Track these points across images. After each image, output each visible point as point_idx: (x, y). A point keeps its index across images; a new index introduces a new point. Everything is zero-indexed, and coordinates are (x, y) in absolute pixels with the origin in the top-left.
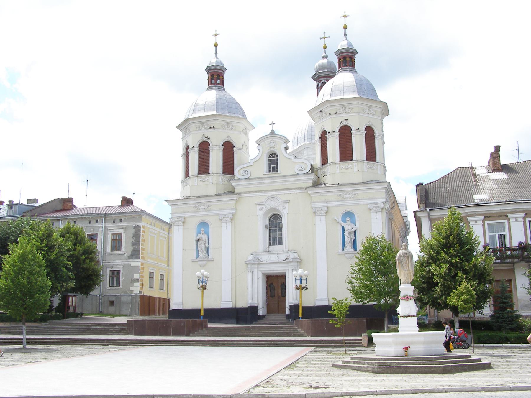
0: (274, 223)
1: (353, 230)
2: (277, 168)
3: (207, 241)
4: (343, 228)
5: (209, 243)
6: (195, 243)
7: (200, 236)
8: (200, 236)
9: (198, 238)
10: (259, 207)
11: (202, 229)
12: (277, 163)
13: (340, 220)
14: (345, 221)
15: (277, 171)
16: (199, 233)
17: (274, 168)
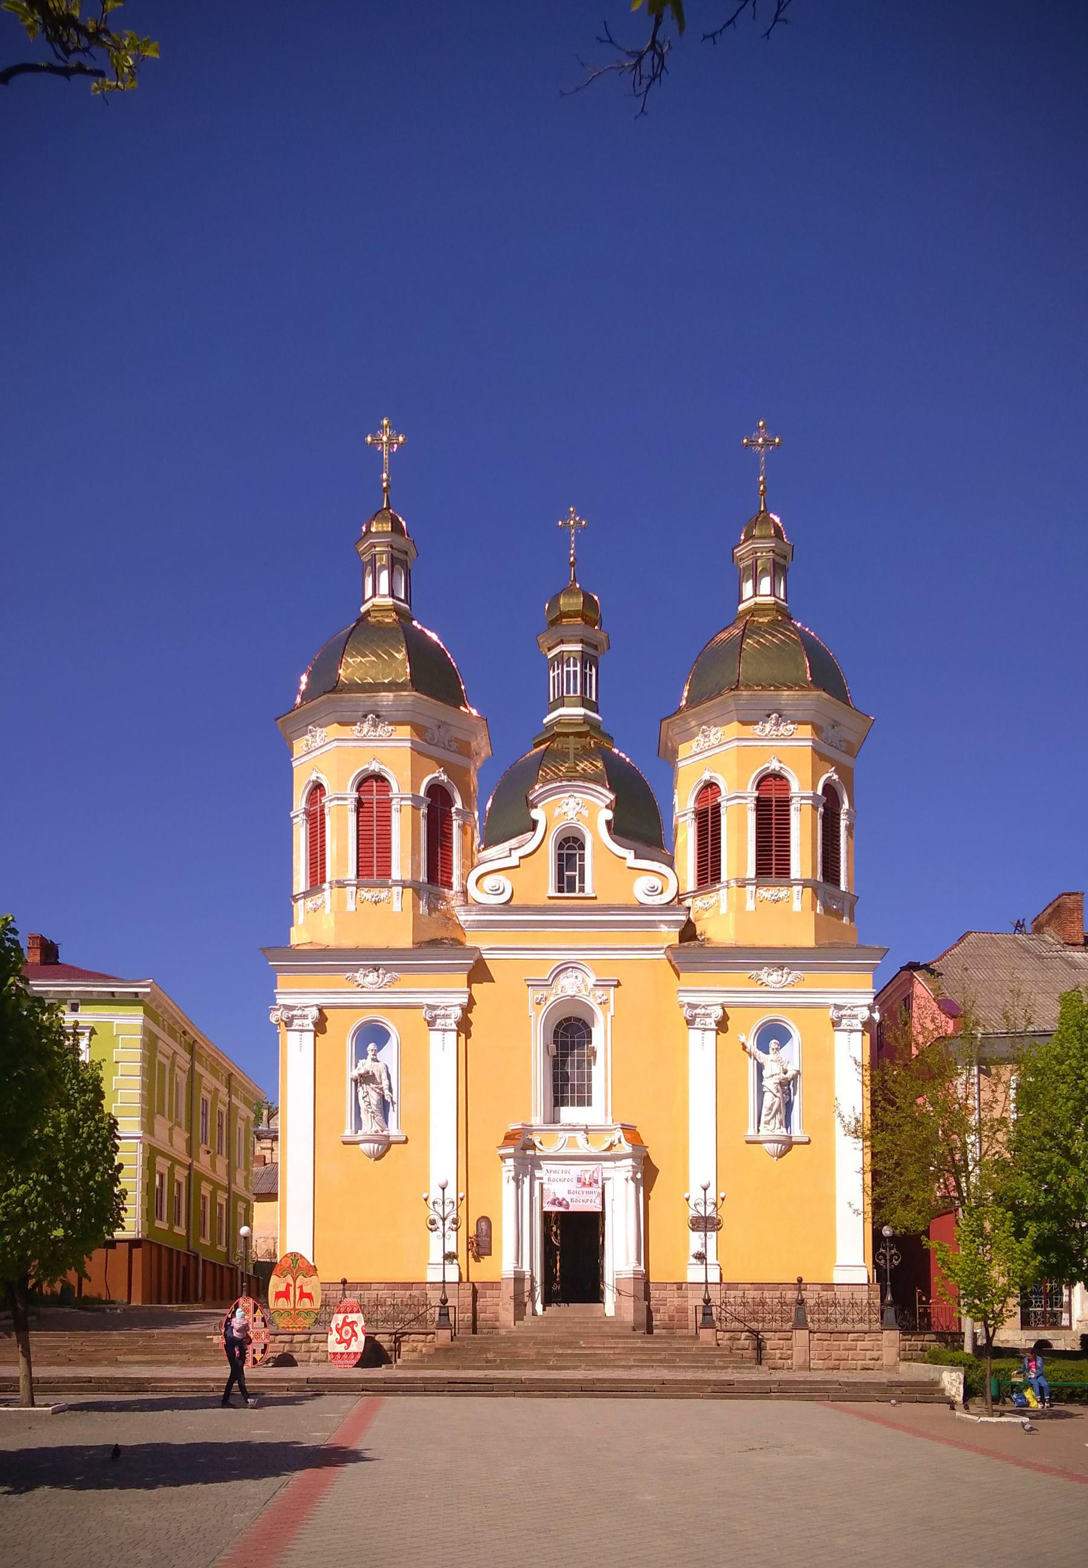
0: (570, 1034)
1: (789, 1075)
2: (582, 881)
3: (385, 1083)
4: (760, 1067)
5: (390, 1089)
6: (349, 1086)
7: (366, 1065)
8: (366, 1065)
9: (362, 1071)
10: (533, 995)
11: (371, 1046)
12: (582, 867)
13: (752, 1045)
14: (767, 1053)
15: (582, 890)
16: (361, 1054)
17: (572, 879)
